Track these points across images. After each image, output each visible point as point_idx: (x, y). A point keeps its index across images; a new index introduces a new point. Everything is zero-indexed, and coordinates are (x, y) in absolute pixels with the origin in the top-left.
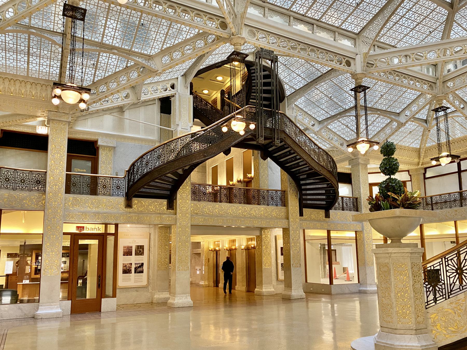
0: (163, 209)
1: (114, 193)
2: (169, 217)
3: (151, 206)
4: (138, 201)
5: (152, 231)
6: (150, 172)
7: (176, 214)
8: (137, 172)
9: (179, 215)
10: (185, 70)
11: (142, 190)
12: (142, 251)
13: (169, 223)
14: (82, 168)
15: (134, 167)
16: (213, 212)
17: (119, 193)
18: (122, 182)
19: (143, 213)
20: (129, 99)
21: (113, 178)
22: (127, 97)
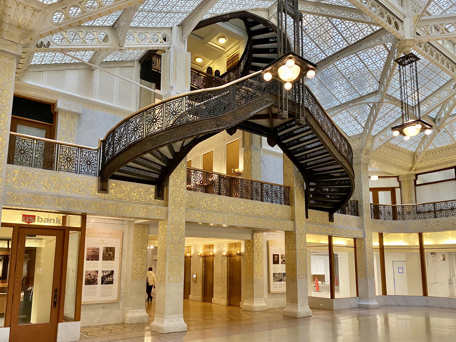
0: (150, 198)
2: (158, 209)
3: (134, 193)
4: (117, 185)
5: (126, 229)
7: (167, 205)
8: (119, 140)
10: (185, 16)
12: (112, 255)
13: (157, 217)
14: (32, 134)
16: (211, 207)
17: (90, 171)
18: (94, 155)
20: (107, 43)
21: (81, 148)
22: (105, 39)
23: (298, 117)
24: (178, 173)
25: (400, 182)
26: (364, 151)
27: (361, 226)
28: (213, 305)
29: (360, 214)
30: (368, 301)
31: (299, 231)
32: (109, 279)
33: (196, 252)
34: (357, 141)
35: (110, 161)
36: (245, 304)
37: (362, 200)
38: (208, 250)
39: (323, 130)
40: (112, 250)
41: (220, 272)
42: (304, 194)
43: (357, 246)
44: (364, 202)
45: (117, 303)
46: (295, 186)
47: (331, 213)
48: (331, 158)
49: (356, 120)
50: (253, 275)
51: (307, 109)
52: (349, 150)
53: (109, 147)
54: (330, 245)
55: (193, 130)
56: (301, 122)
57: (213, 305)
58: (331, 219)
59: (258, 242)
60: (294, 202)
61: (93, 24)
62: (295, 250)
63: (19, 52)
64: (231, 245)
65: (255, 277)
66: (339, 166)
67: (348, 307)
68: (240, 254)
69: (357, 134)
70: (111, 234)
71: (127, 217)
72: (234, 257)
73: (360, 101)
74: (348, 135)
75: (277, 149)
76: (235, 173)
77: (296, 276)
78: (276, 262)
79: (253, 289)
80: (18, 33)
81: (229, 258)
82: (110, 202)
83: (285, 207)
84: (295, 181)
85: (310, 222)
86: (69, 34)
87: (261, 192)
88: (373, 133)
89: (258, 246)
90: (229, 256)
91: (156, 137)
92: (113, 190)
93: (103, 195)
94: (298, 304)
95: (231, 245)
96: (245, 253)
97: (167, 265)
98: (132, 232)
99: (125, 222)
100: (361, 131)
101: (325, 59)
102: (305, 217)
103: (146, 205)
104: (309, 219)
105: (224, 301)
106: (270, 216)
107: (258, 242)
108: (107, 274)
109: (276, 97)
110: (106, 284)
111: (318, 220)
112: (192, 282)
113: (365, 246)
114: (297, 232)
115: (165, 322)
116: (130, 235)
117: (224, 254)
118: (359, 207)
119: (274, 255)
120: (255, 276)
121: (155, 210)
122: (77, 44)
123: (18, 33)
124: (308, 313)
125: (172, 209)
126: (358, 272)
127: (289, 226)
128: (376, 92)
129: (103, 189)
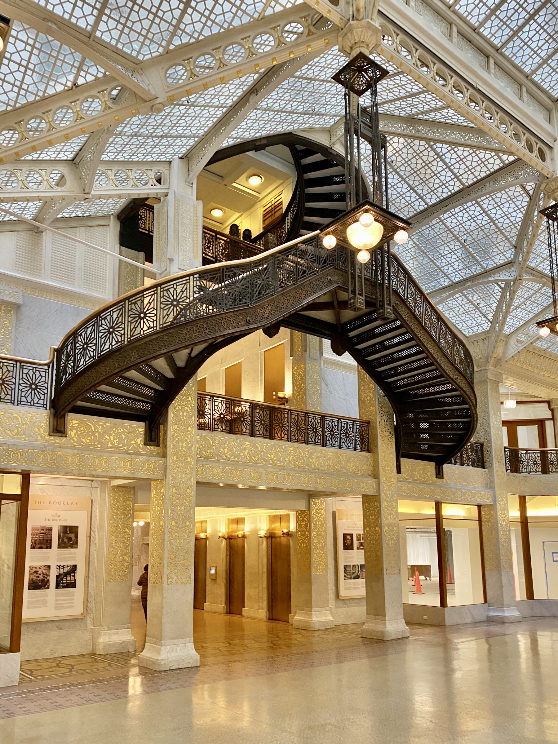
0: (136, 443)
1: (24, 399)
3: (110, 435)
4: (81, 422)
5: (97, 495)
6: (118, 350)
7: (164, 455)
8: (84, 349)
9: (171, 459)
11: (92, 394)
12: (73, 539)
13: (148, 475)
15: (74, 339)
16: (238, 456)
17: (36, 400)
19: (91, 450)
21: (21, 362)
23: (382, 306)
24: (183, 401)
25: (552, 410)
26: (492, 361)
27: (490, 485)
28: (244, 620)
29: (487, 464)
30: (503, 611)
31: (386, 495)
32: (68, 579)
33: (215, 532)
34: (481, 343)
35: (69, 383)
36: (297, 617)
37: (490, 442)
38: (235, 526)
39: (423, 327)
40: (74, 530)
41: (256, 562)
42: (393, 433)
43: (483, 518)
44: (493, 444)
45: (82, 619)
46: (378, 419)
47: (439, 462)
48: (437, 373)
49: (478, 309)
50: (310, 568)
51: (396, 293)
52: (466, 360)
53: (67, 361)
54: (438, 517)
55: (207, 331)
56: (387, 315)
57: (244, 620)
58: (439, 474)
59: (318, 513)
60: (377, 446)
62: (380, 527)
64: (272, 519)
65: (314, 573)
66: (450, 387)
67: (469, 620)
68: (288, 534)
69: (479, 331)
70: (72, 503)
71: (97, 476)
72: (278, 539)
73: (484, 277)
74: (465, 333)
75: (347, 358)
76: (279, 398)
77: (382, 570)
78: (348, 546)
79: (310, 592)
81: (269, 539)
82: (70, 451)
83: (362, 456)
84: (378, 412)
85: (404, 480)
87: (322, 431)
88: (507, 330)
89: (319, 520)
90: (271, 536)
91: (146, 343)
92: (75, 431)
93: (58, 440)
94: (387, 617)
95: (272, 519)
96: (297, 532)
97: (166, 555)
98: (107, 499)
99: (95, 484)
100: (487, 326)
101: (425, 210)
102: (395, 470)
103: (129, 456)
104: (404, 474)
105: (263, 614)
106: (338, 471)
107: (318, 513)
108: (65, 571)
109: (344, 274)
110: (63, 587)
111: (417, 475)
112: (208, 581)
113: (496, 518)
114: (382, 495)
115: (162, 653)
116: (104, 504)
117: (262, 533)
118: (485, 453)
119: (345, 535)
120: (313, 569)
121: (145, 463)
124: (403, 632)
125: (173, 460)
126: (485, 561)
127: (369, 486)
128: (509, 264)
129: (58, 429)
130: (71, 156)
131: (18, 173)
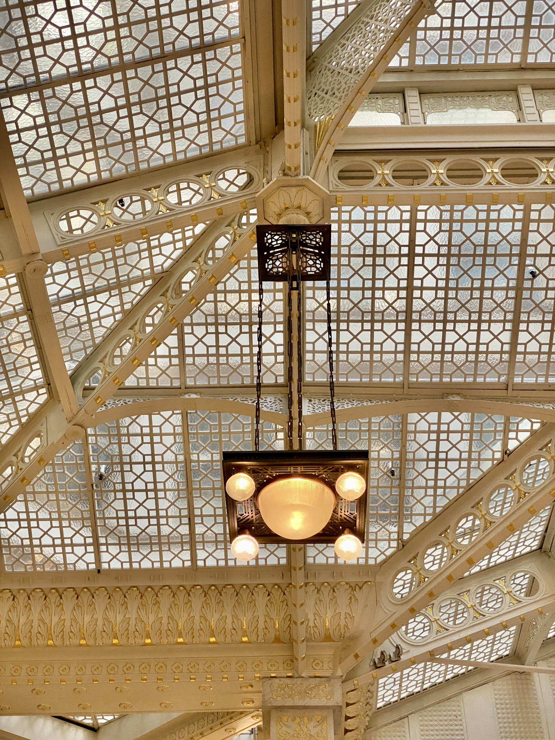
61: (489, 562)
63: (337, 699)
80: (327, 652)
86: (442, 611)
122: (465, 625)
123: (327, 652)
130: (535, 544)
131: (465, 598)
